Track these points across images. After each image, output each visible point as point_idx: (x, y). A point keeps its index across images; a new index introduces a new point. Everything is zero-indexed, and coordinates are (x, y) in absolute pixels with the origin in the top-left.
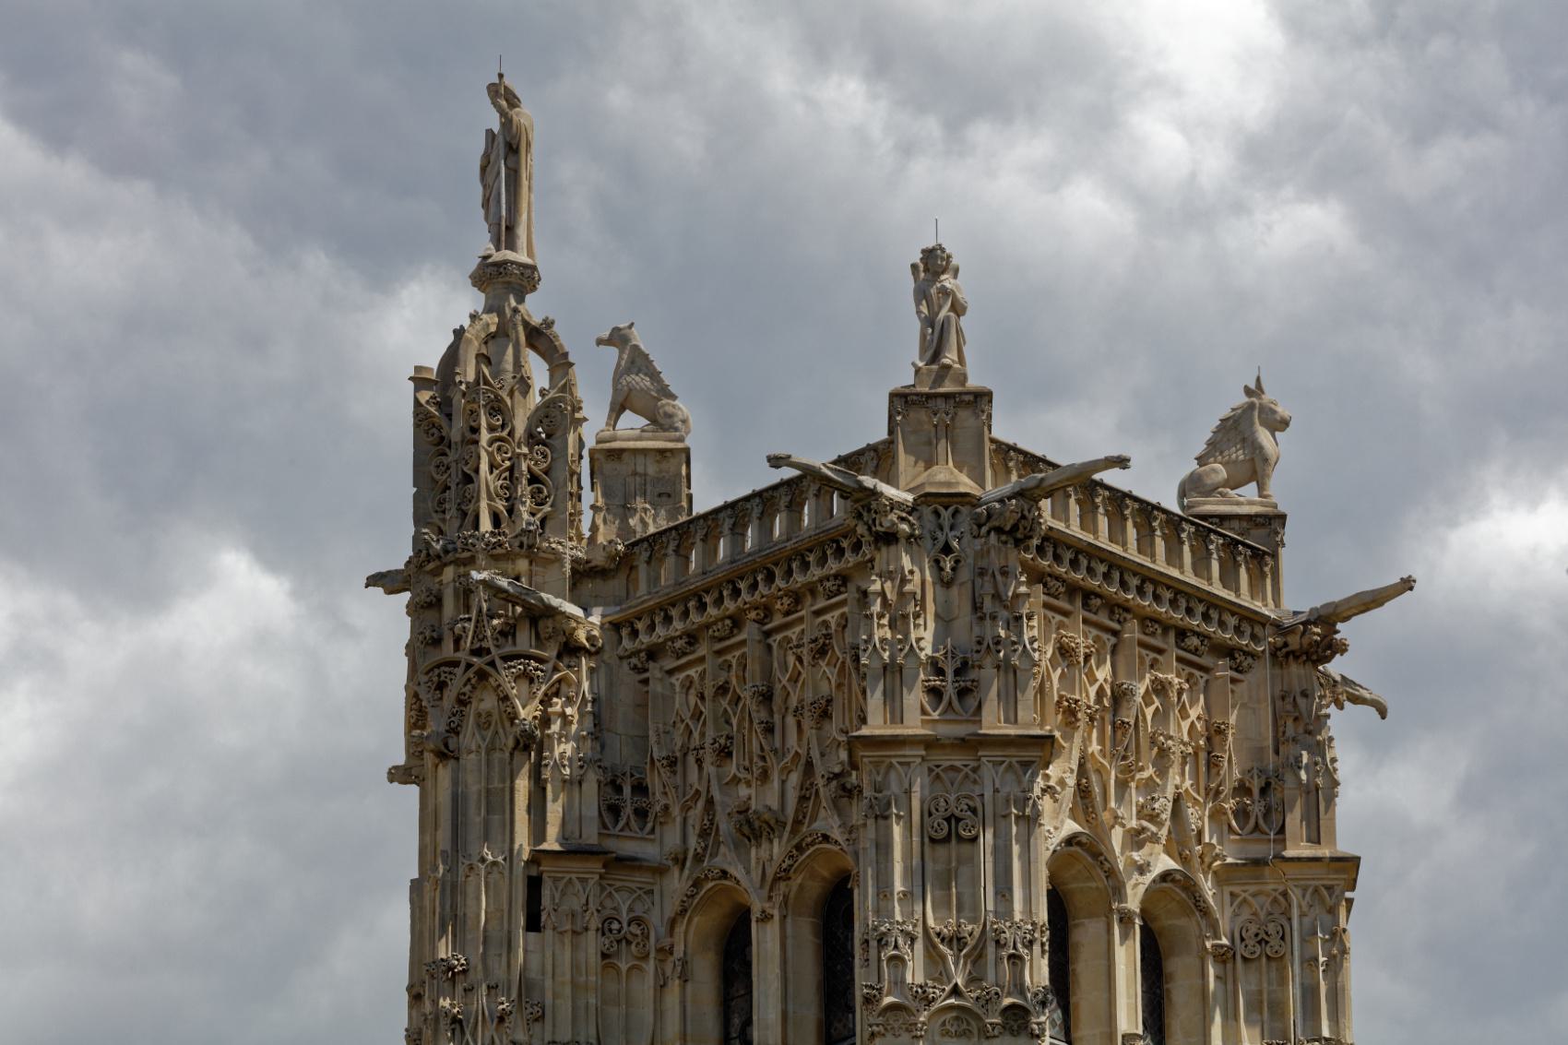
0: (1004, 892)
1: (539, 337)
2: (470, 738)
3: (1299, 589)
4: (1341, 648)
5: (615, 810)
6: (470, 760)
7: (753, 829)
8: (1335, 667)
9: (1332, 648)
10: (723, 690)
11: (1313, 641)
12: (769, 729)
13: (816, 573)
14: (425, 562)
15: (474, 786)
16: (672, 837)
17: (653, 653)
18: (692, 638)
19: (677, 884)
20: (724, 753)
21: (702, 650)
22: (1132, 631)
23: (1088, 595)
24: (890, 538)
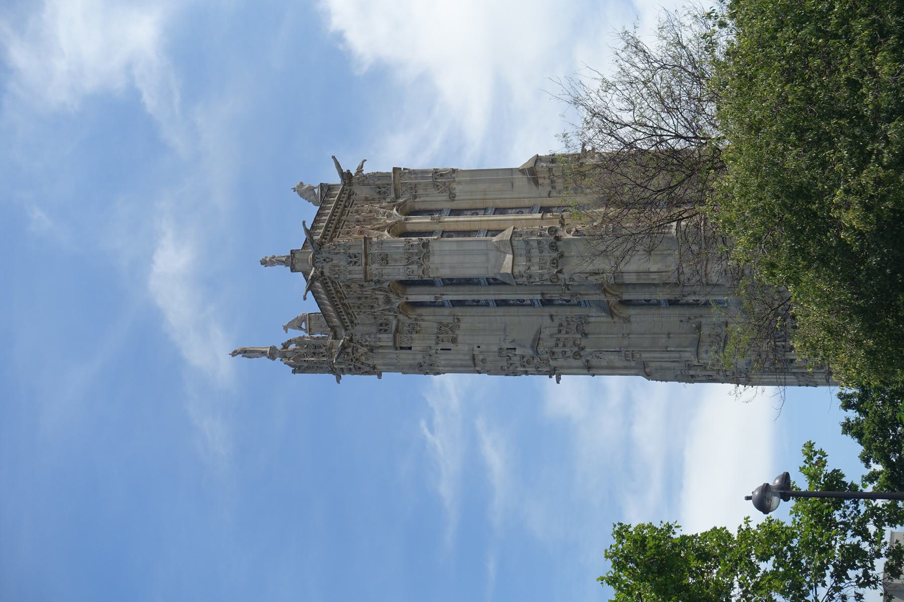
0: (398, 248)
1: (285, 346)
2: (370, 362)
3: (335, 179)
4: (348, 171)
5: (386, 331)
6: (376, 362)
7: (388, 301)
8: (353, 172)
9: (349, 172)
10: (359, 307)
11: (346, 177)
12: (366, 298)
13: (332, 288)
14: (333, 371)
15: (380, 361)
16: (391, 318)
17: (352, 322)
18: (348, 314)
19: (401, 317)
20: (372, 307)
21: (350, 311)
22: (344, 218)
23: (336, 228)
24: (322, 273)
